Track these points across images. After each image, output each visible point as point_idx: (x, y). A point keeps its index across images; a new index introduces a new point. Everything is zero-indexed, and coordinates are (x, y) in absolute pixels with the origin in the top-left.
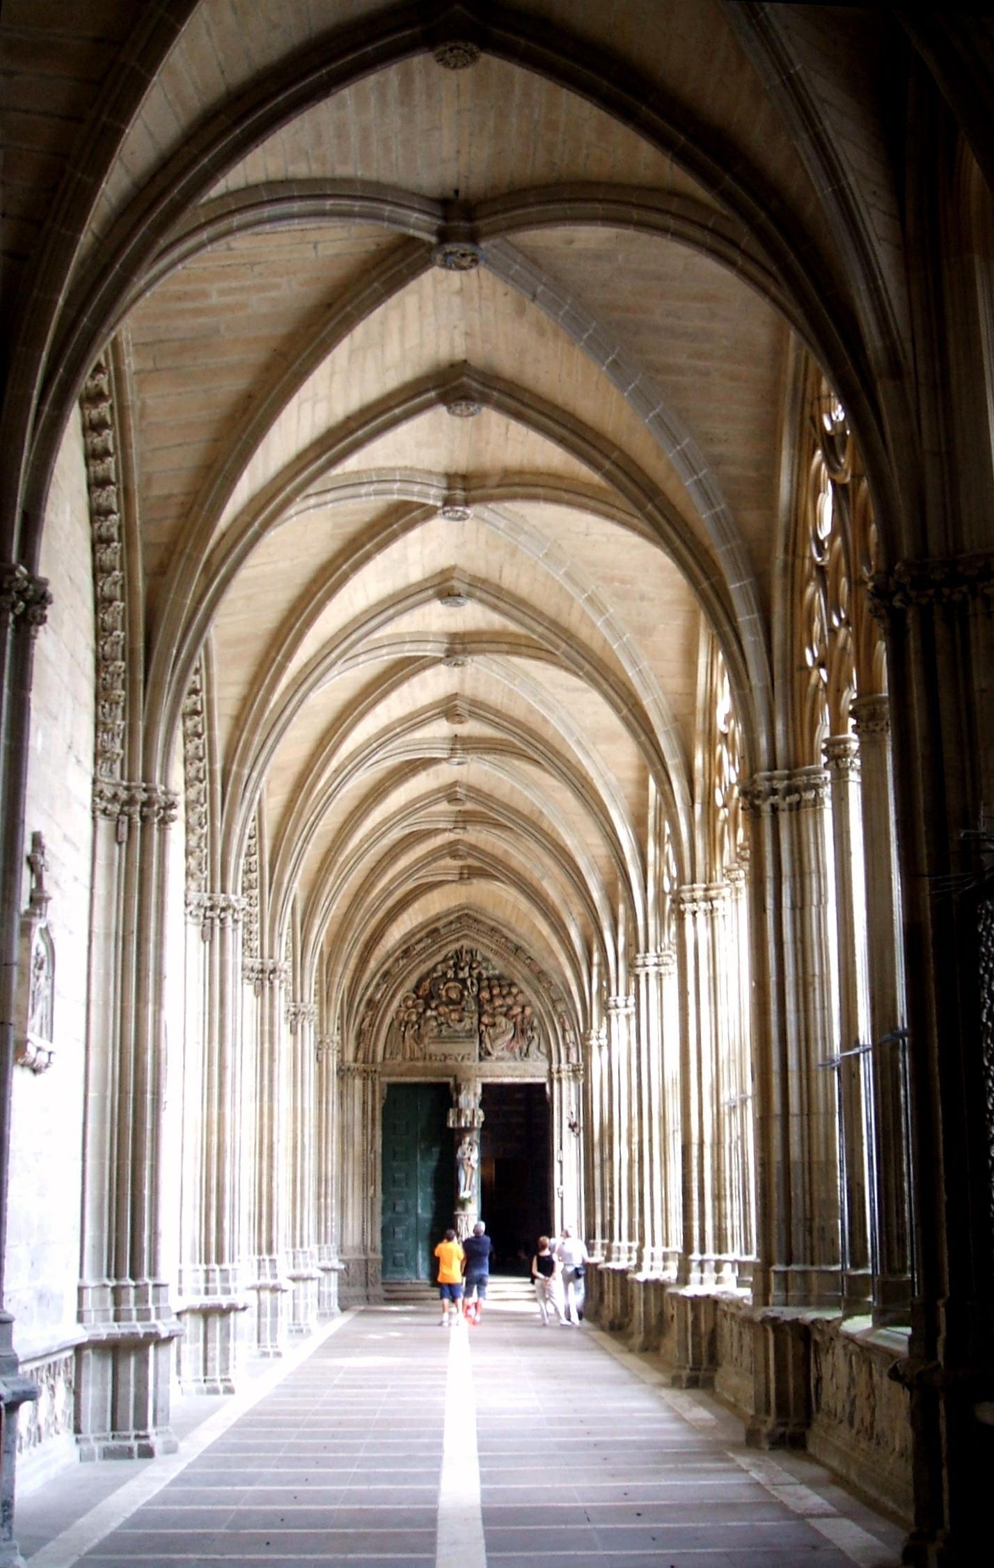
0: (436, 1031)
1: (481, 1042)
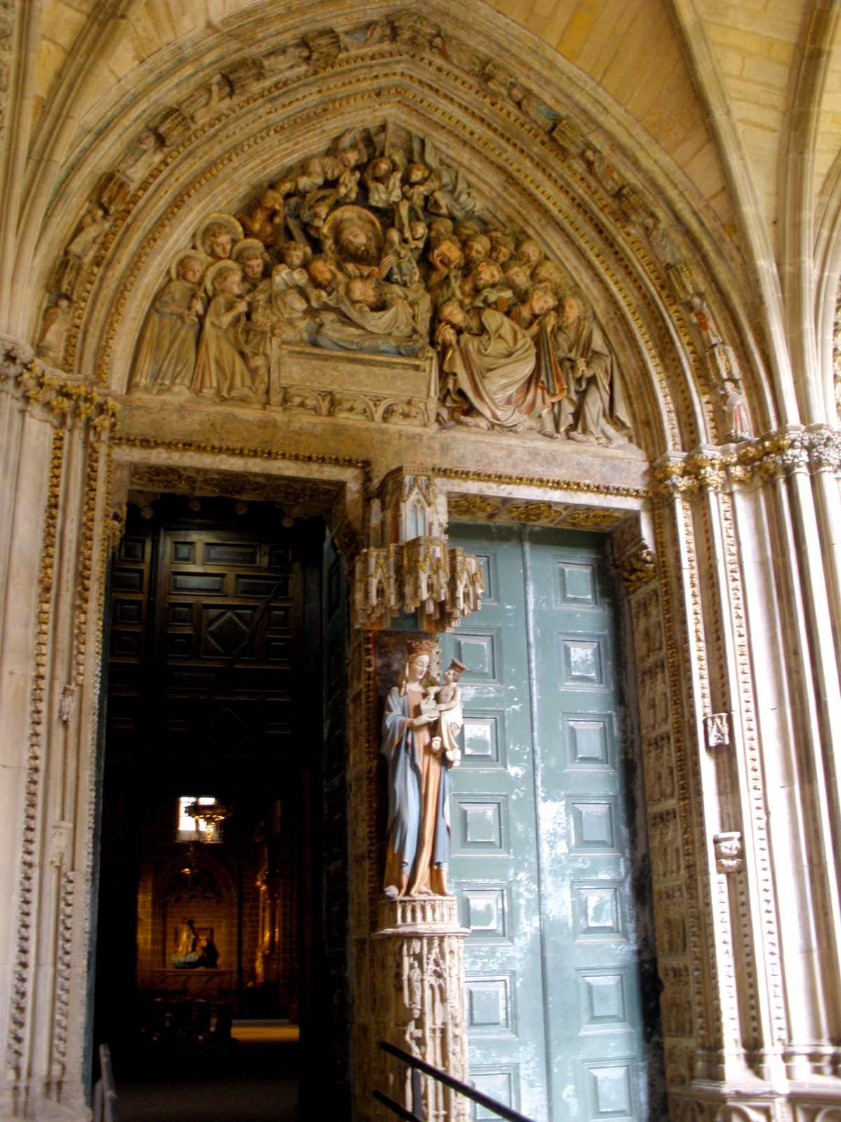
0: (303, 324)
1: (443, 375)
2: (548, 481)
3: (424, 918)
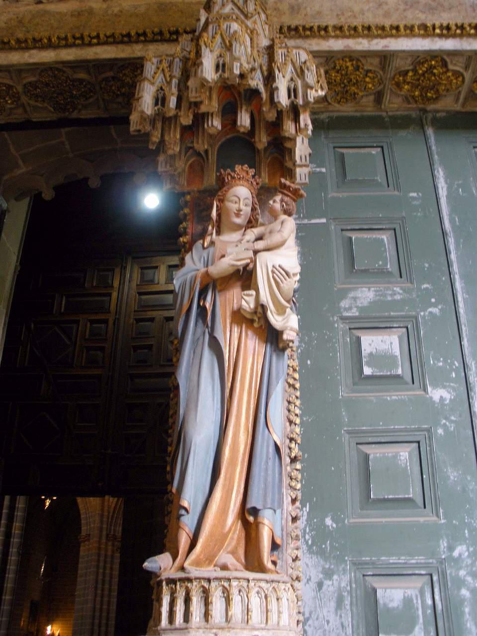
2: (434, 28)
3: (207, 615)
